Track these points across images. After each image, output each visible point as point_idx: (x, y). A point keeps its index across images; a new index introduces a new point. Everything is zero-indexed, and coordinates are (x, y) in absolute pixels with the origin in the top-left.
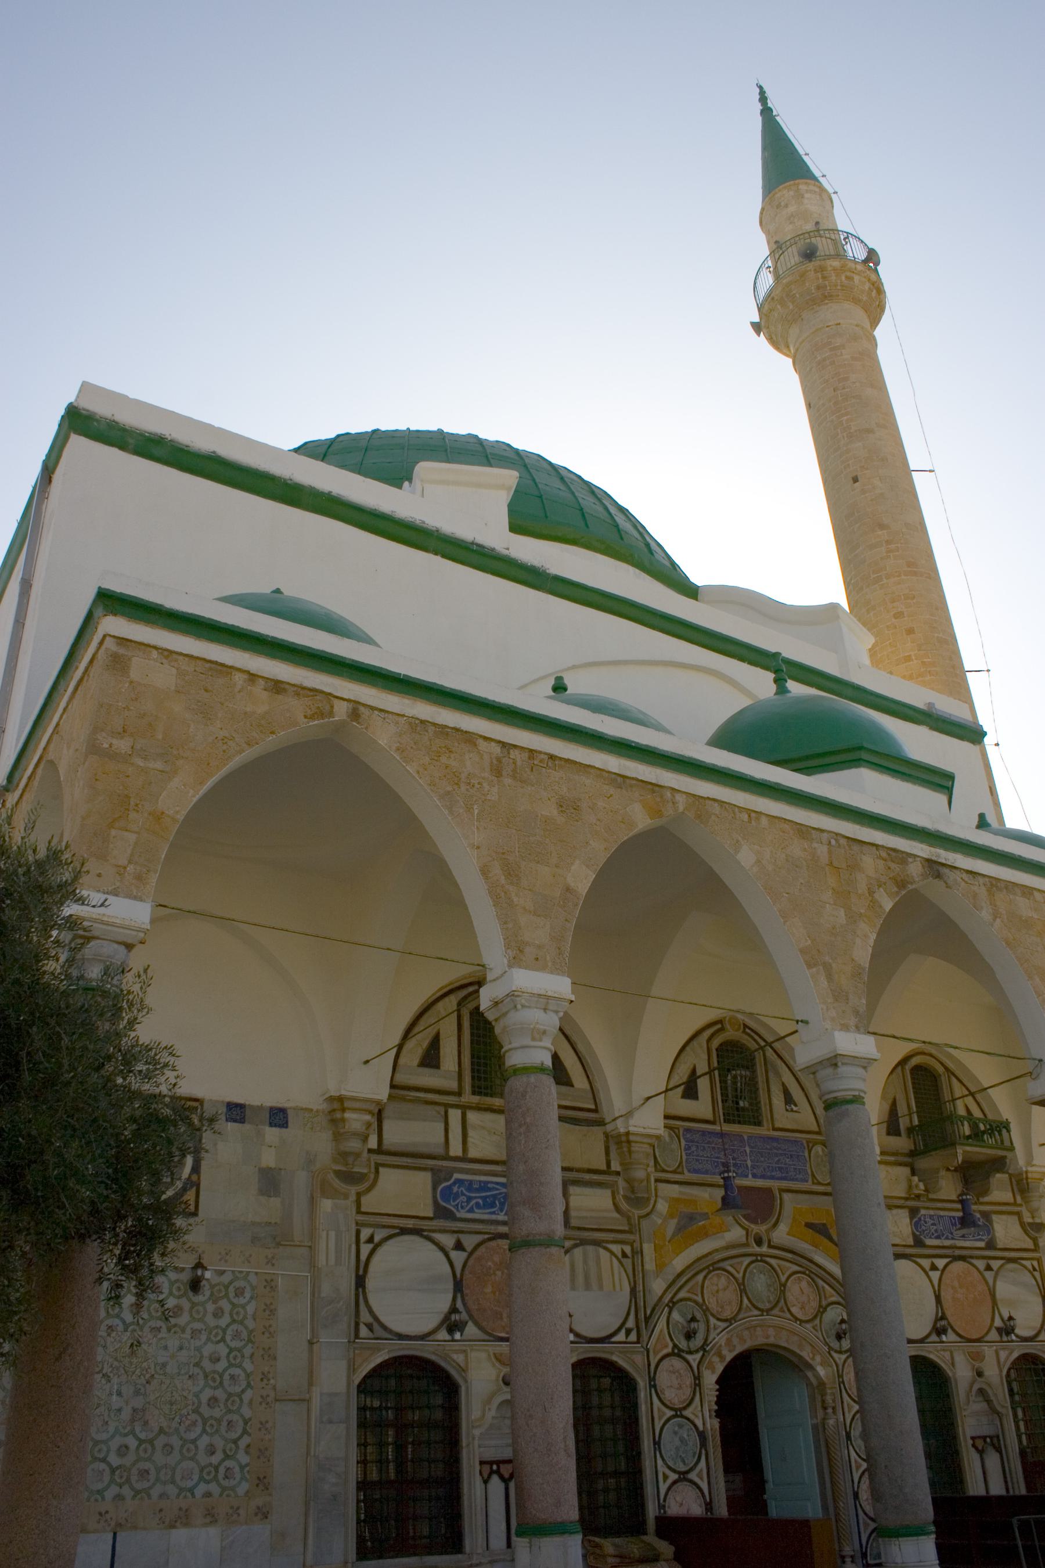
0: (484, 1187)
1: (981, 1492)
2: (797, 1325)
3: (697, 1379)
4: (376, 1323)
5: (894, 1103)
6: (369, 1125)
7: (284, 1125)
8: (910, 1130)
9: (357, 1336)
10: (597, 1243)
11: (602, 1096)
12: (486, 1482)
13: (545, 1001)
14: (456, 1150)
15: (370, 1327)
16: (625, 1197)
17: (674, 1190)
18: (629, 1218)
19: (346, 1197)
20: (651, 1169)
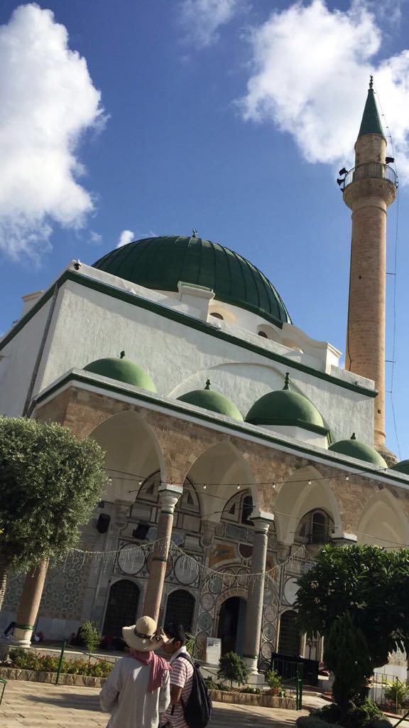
1: (303, 657)
7: (103, 507)
8: (309, 536)
10: (191, 555)
14: (153, 520)
17: (220, 542)
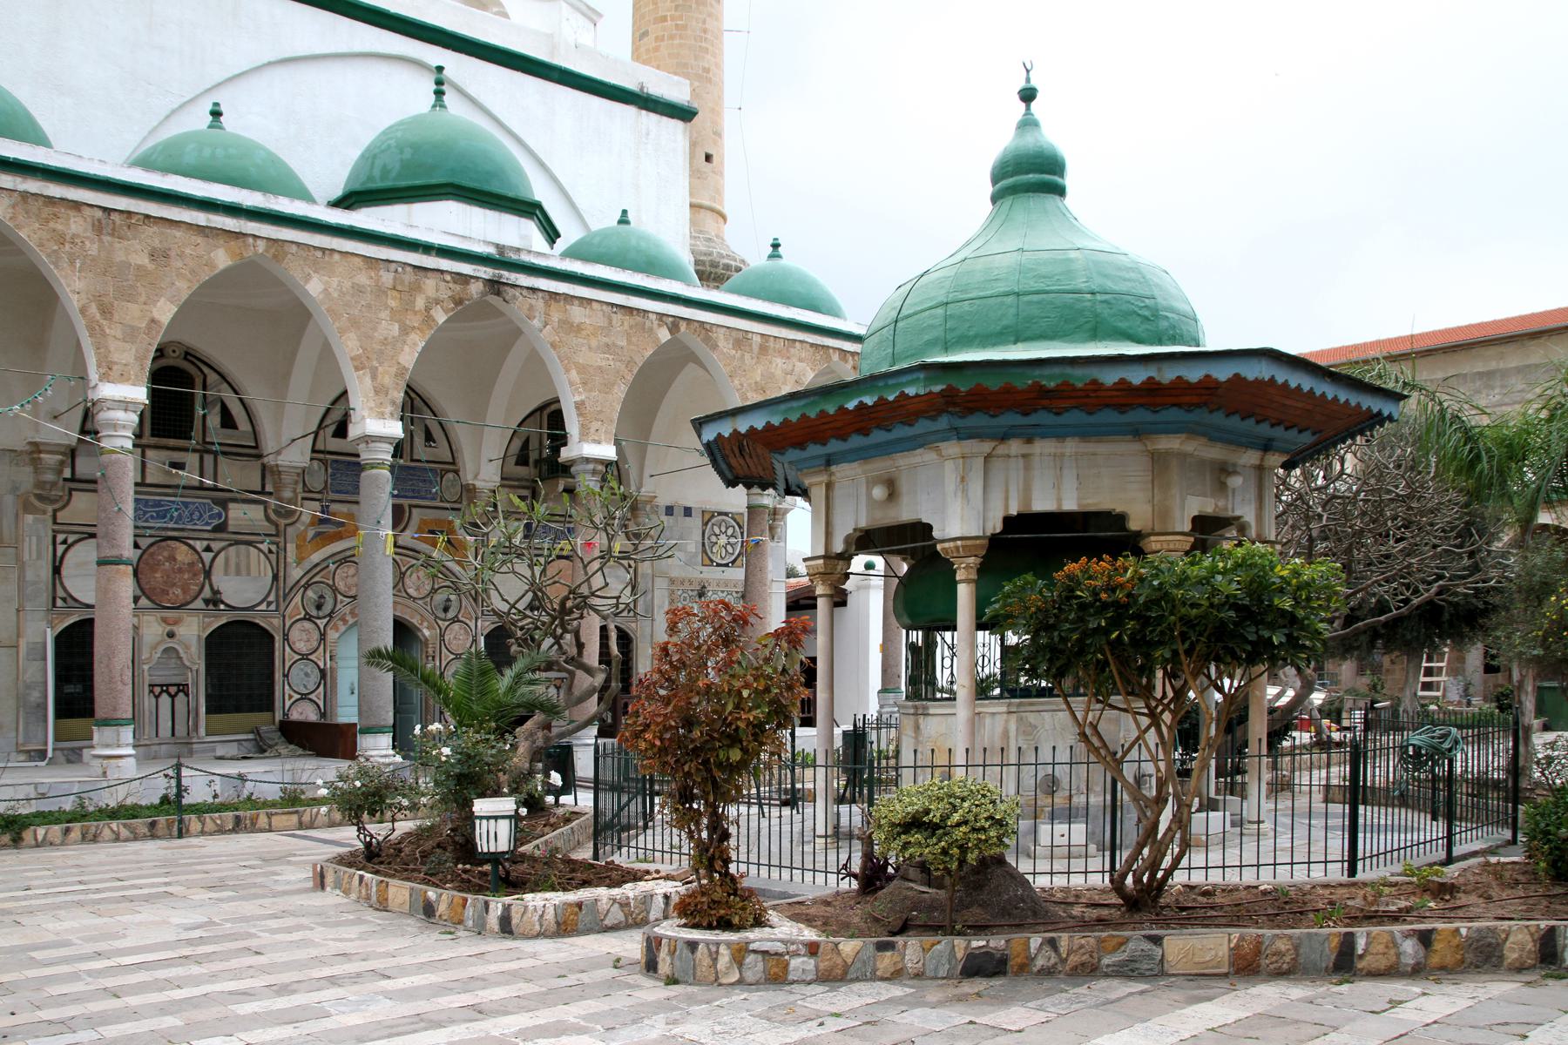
0: (158, 504)
2: (410, 603)
3: (323, 637)
4: (69, 598)
5: (527, 441)
6: (62, 463)
9: (54, 605)
10: (249, 543)
11: (262, 437)
12: (157, 697)
13: (125, 405)
15: (64, 600)
16: (276, 512)
18: (277, 526)
19: (44, 512)
20: (300, 488)
